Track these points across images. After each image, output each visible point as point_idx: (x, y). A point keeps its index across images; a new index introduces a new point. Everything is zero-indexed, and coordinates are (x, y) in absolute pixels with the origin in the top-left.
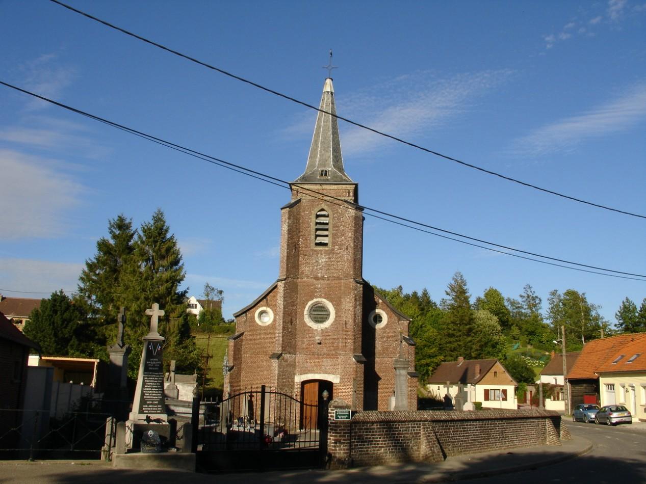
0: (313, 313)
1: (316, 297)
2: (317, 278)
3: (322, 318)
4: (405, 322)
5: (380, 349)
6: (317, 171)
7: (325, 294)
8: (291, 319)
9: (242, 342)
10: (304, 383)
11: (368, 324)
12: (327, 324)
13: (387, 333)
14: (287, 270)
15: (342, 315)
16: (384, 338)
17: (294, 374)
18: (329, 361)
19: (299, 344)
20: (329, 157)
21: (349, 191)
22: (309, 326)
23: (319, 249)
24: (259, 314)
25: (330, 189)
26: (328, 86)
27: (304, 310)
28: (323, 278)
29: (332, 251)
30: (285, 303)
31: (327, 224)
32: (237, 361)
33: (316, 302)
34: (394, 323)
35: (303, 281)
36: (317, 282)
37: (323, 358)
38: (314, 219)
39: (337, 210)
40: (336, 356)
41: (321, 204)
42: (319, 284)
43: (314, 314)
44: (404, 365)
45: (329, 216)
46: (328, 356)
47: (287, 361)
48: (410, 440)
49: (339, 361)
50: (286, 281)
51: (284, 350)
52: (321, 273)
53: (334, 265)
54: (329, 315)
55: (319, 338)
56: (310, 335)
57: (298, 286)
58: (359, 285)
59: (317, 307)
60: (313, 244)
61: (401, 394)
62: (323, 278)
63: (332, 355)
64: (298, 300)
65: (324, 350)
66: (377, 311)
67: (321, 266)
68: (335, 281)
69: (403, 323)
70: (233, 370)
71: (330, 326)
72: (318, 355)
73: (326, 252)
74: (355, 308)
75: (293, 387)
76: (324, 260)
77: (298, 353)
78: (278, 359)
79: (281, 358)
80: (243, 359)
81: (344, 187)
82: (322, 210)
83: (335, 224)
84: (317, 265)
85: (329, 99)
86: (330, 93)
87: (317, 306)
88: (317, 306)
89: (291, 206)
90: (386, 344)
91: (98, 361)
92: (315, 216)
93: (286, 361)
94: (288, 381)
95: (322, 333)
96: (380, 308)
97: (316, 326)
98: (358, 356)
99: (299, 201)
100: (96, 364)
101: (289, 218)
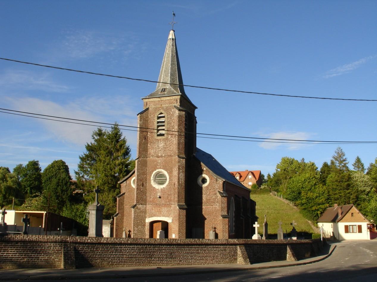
0: (157, 179)
1: (158, 169)
2: (158, 157)
3: (163, 182)
4: (221, 182)
5: (205, 200)
6: (160, 89)
7: (163, 166)
8: (143, 183)
9: (124, 198)
10: (152, 224)
11: (198, 184)
12: (164, 186)
13: (209, 189)
14: (139, 153)
15: (173, 179)
16: (208, 193)
17: (146, 217)
18: (166, 209)
19: (148, 198)
20: (168, 80)
21: (177, 100)
22: (154, 187)
23: (159, 138)
24: (133, 183)
25: (166, 100)
26: (171, 35)
27: (151, 177)
28: (162, 156)
29: (167, 139)
30: (138, 173)
31: (164, 122)
32: (121, 210)
33: (158, 172)
34: (214, 182)
35: (150, 159)
36: (158, 159)
37: (162, 207)
38: (156, 120)
39: (170, 112)
40: (169, 205)
41: (161, 110)
42: (159, 160)
43: (158, 179)
44: (94, 207)
45: (165, 117)
46: (165, 205)
47: (140, 209)
48: (51, 254)
49: (172, 208)
50: (139, 159)
51: (138, 202)
52: (161, 153)
53: (168, 147)
54: (166, 179)
55: (159, 194)
56: (155, 192)
57: (147, 162)
58: (181, 159)
59: (159, 175)
60: (156, 135)
61: (92, 226)
62: (162, 156)
63: (168, 205)
64: (148, 171)
65: (162, 201)
66: (204, 175)
67: (160, 149)
68: (169, 158)
69: (220, 183)
70: (118, 216)
71: (166, 186)
72: (159, 205)
73: (163, 139)
74: (179, 174)
75: (144, 225)
76: (162, 145)
77: (147, 204)
78: (133, 208)
79: (135, 208)
80: (125, 209)
81: (174, 97)
82: (161, 113)
83: (169, 121)
84: (158, 148)
85: (170, 43)
86: (171, 39)
87: (159, 174)
88: (159, 174)
89: (141, 113)
90: (209, 197)
91: (46, 212)
92: (157, 117)
93: (140, 209)
94: (141, 222)
95: (162, 191)
96: (205, 174)
97: (158, 187)
98: (181, 205)
99: (148, 109)
100: (44, 214)
101: (140, 121)
